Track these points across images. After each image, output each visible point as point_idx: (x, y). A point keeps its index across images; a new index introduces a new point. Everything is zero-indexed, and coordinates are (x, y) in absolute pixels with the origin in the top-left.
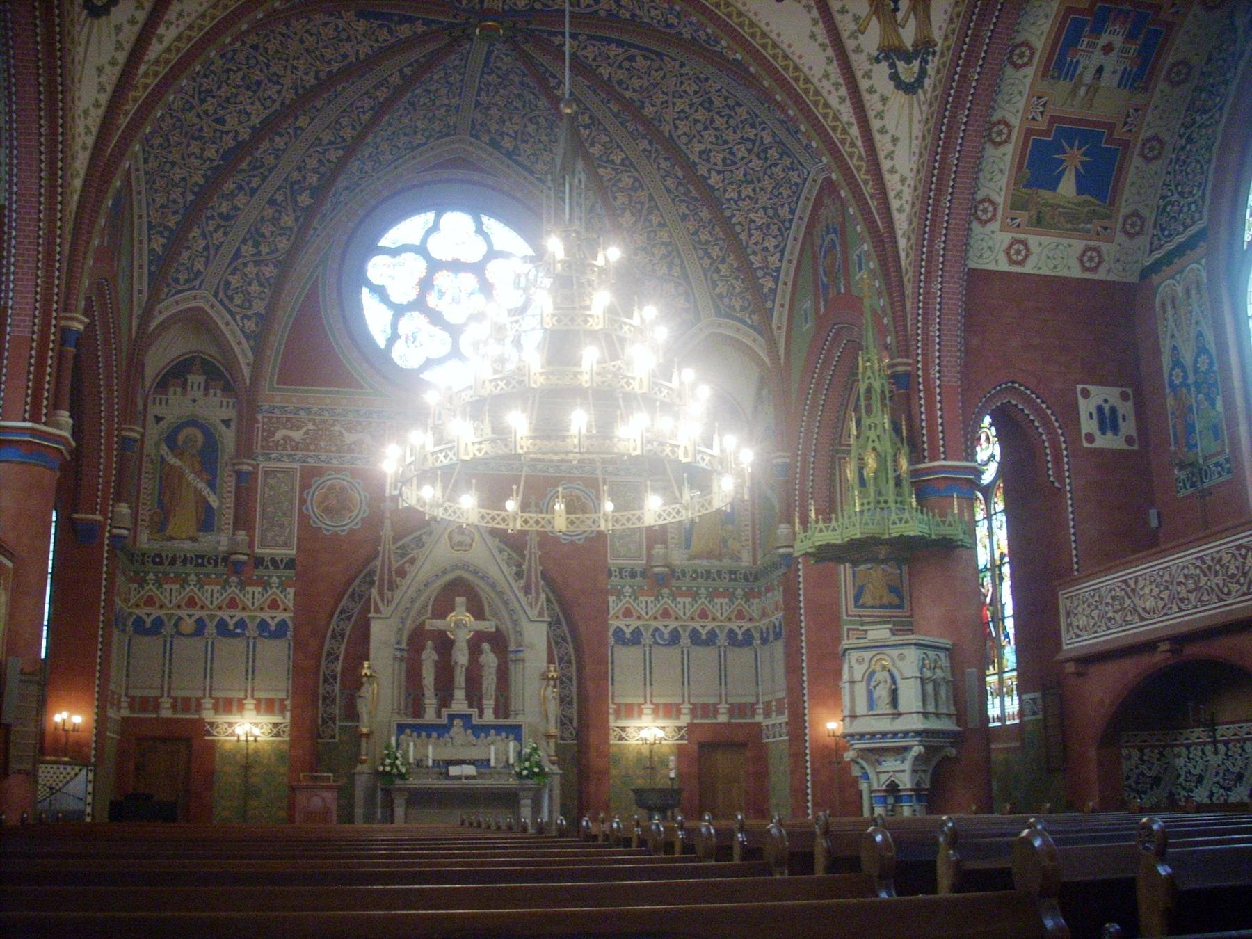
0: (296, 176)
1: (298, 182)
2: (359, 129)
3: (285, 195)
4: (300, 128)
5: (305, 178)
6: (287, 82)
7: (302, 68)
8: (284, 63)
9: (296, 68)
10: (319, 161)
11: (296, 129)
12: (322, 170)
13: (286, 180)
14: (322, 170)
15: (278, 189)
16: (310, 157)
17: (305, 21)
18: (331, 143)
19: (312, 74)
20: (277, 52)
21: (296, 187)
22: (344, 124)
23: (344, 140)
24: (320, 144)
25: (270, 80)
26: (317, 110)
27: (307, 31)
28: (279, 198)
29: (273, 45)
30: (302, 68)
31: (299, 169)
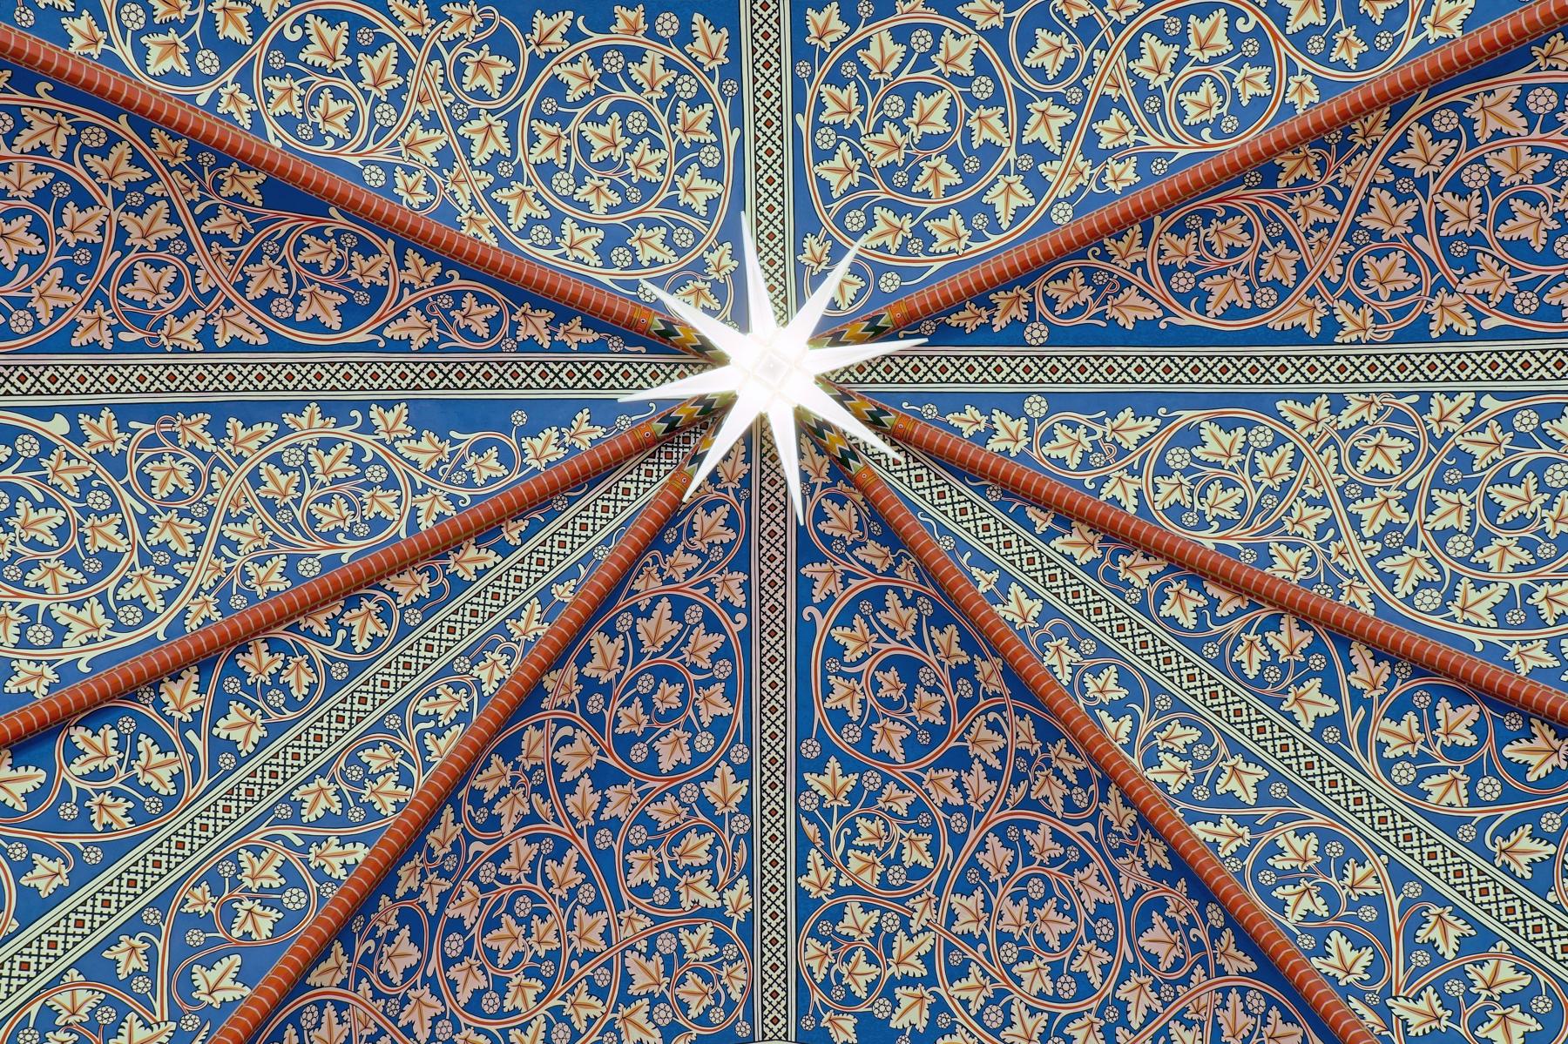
0: (199, 900)
1: (204, 923)
2: (420, 780)
3: (151, 955)
4: (230, 745)
5: (229, 914)
6: (202, 573)
7: (246, 546)
8: (197, 528)
9: (234, 546)
10: (285, 870)
11: (220, 746)
12: (294, 899)
13: (162, 902)
14: (294, 899)
15: (133, 926)
16: (257, 851)
17: (270, 429)
18: (328, 819)
19: (279, 563)
20: (178, 494)
21: (195, 937)
22: (375, 766)
23: (372, 813)
24: (296, 820)
25: (145, 560)
26: (292, 703)
27: (276, 459)
28: (127, 959)
29: (169, 476)
30: (246, 546)
31: (214, 881)
